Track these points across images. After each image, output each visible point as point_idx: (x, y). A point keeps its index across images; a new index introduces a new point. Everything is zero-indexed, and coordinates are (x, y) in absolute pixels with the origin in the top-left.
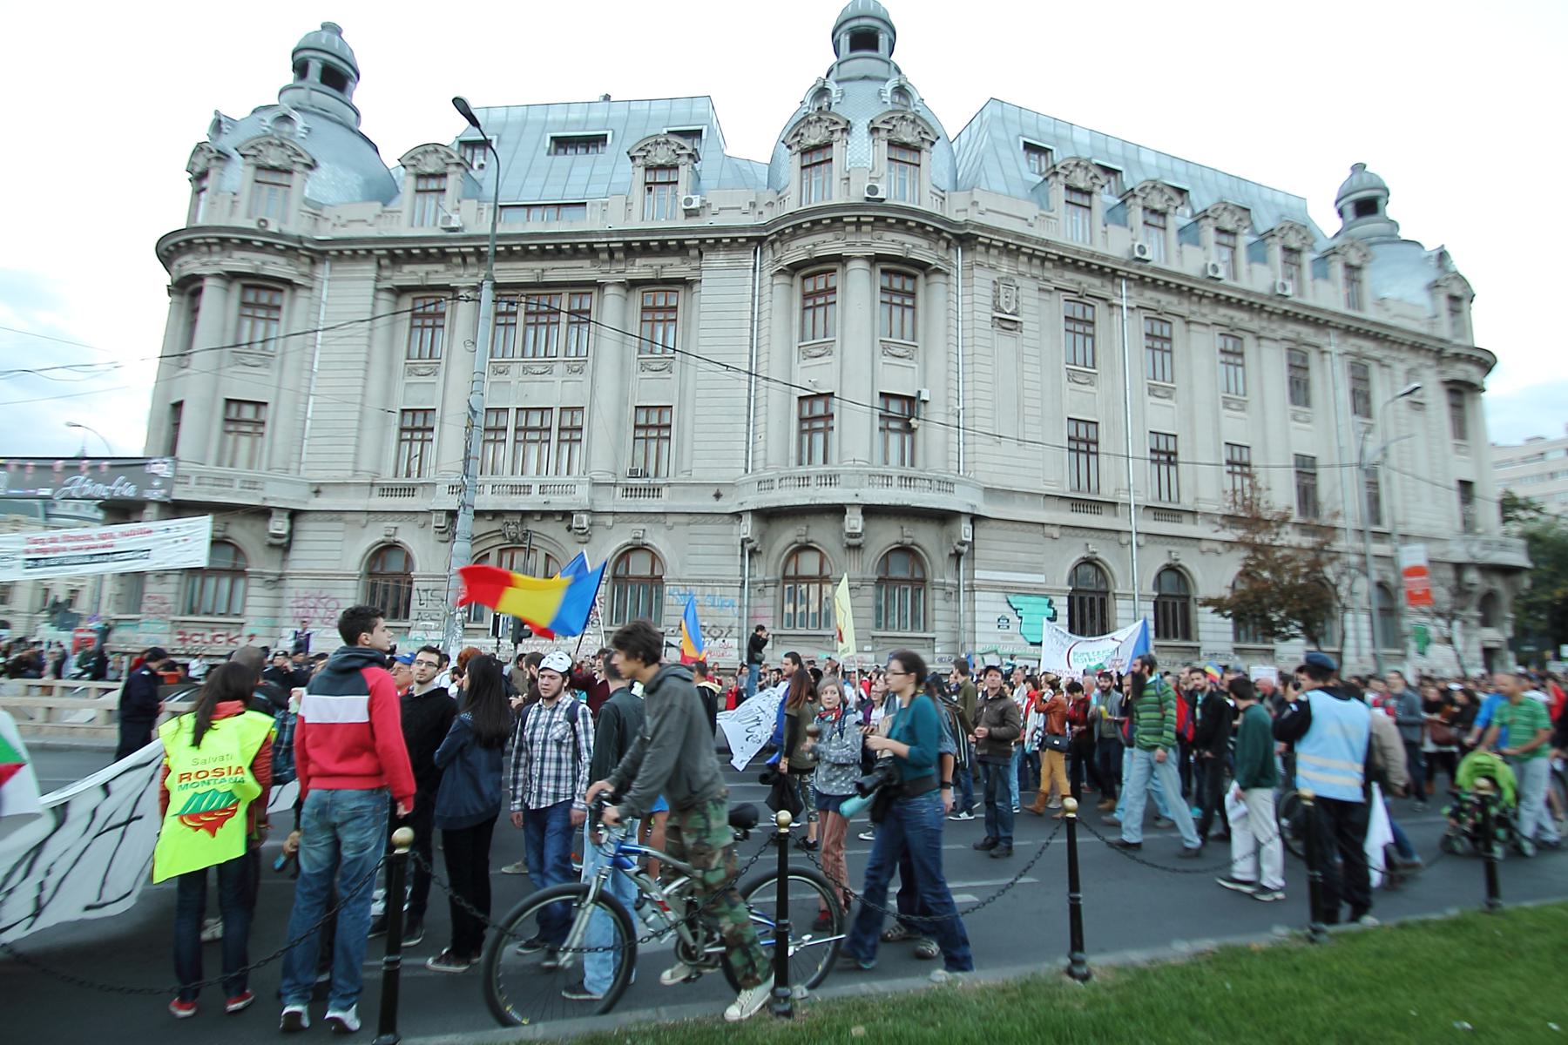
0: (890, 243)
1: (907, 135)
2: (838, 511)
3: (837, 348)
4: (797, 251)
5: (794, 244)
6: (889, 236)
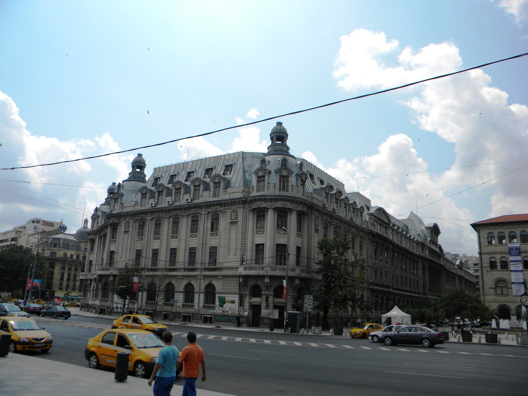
0: (279, 204)
1: (285, 173)
2: (263, 277)
3: (265, 233)
4: (255, 205)
5: (255, 203)
6: (279, 202)
